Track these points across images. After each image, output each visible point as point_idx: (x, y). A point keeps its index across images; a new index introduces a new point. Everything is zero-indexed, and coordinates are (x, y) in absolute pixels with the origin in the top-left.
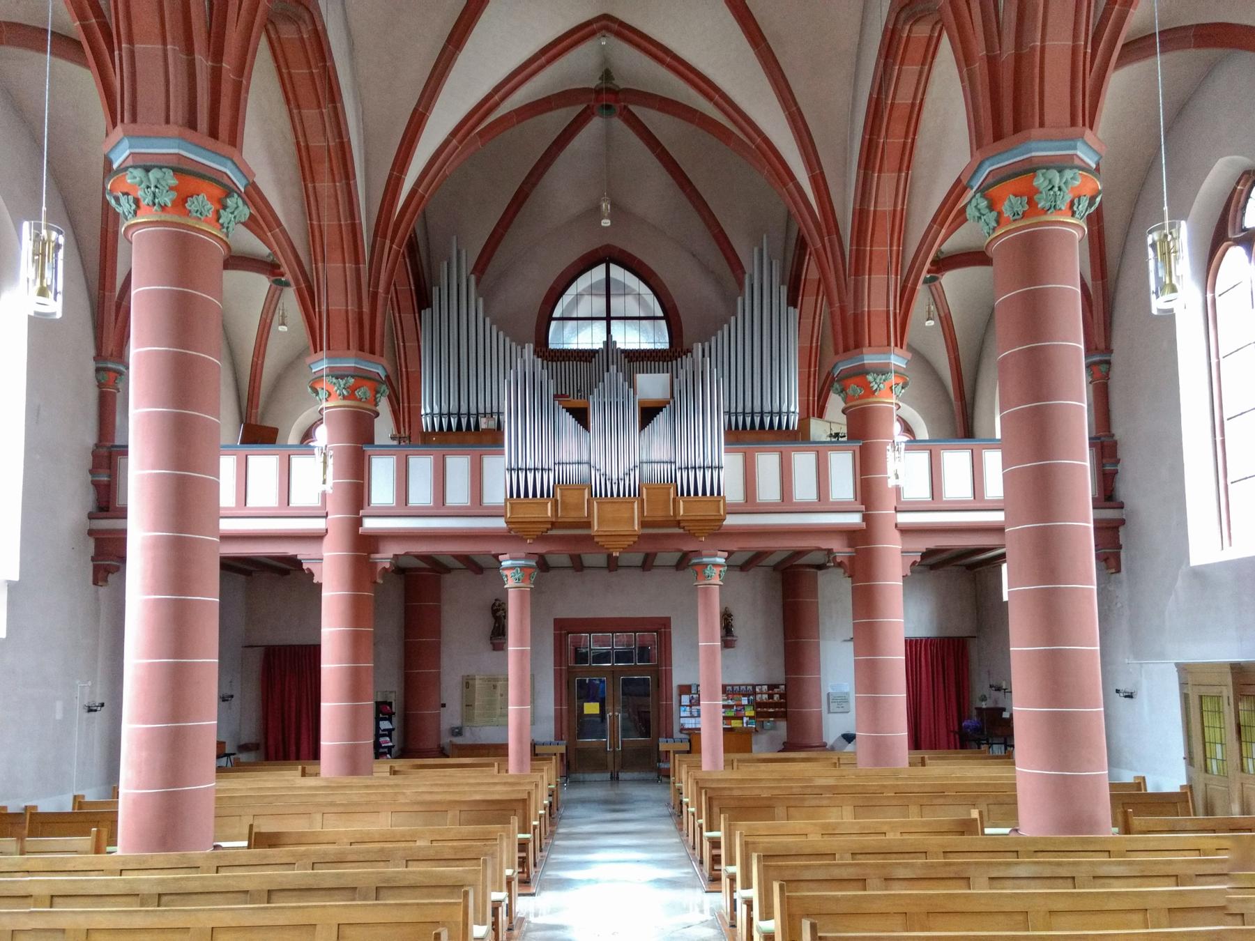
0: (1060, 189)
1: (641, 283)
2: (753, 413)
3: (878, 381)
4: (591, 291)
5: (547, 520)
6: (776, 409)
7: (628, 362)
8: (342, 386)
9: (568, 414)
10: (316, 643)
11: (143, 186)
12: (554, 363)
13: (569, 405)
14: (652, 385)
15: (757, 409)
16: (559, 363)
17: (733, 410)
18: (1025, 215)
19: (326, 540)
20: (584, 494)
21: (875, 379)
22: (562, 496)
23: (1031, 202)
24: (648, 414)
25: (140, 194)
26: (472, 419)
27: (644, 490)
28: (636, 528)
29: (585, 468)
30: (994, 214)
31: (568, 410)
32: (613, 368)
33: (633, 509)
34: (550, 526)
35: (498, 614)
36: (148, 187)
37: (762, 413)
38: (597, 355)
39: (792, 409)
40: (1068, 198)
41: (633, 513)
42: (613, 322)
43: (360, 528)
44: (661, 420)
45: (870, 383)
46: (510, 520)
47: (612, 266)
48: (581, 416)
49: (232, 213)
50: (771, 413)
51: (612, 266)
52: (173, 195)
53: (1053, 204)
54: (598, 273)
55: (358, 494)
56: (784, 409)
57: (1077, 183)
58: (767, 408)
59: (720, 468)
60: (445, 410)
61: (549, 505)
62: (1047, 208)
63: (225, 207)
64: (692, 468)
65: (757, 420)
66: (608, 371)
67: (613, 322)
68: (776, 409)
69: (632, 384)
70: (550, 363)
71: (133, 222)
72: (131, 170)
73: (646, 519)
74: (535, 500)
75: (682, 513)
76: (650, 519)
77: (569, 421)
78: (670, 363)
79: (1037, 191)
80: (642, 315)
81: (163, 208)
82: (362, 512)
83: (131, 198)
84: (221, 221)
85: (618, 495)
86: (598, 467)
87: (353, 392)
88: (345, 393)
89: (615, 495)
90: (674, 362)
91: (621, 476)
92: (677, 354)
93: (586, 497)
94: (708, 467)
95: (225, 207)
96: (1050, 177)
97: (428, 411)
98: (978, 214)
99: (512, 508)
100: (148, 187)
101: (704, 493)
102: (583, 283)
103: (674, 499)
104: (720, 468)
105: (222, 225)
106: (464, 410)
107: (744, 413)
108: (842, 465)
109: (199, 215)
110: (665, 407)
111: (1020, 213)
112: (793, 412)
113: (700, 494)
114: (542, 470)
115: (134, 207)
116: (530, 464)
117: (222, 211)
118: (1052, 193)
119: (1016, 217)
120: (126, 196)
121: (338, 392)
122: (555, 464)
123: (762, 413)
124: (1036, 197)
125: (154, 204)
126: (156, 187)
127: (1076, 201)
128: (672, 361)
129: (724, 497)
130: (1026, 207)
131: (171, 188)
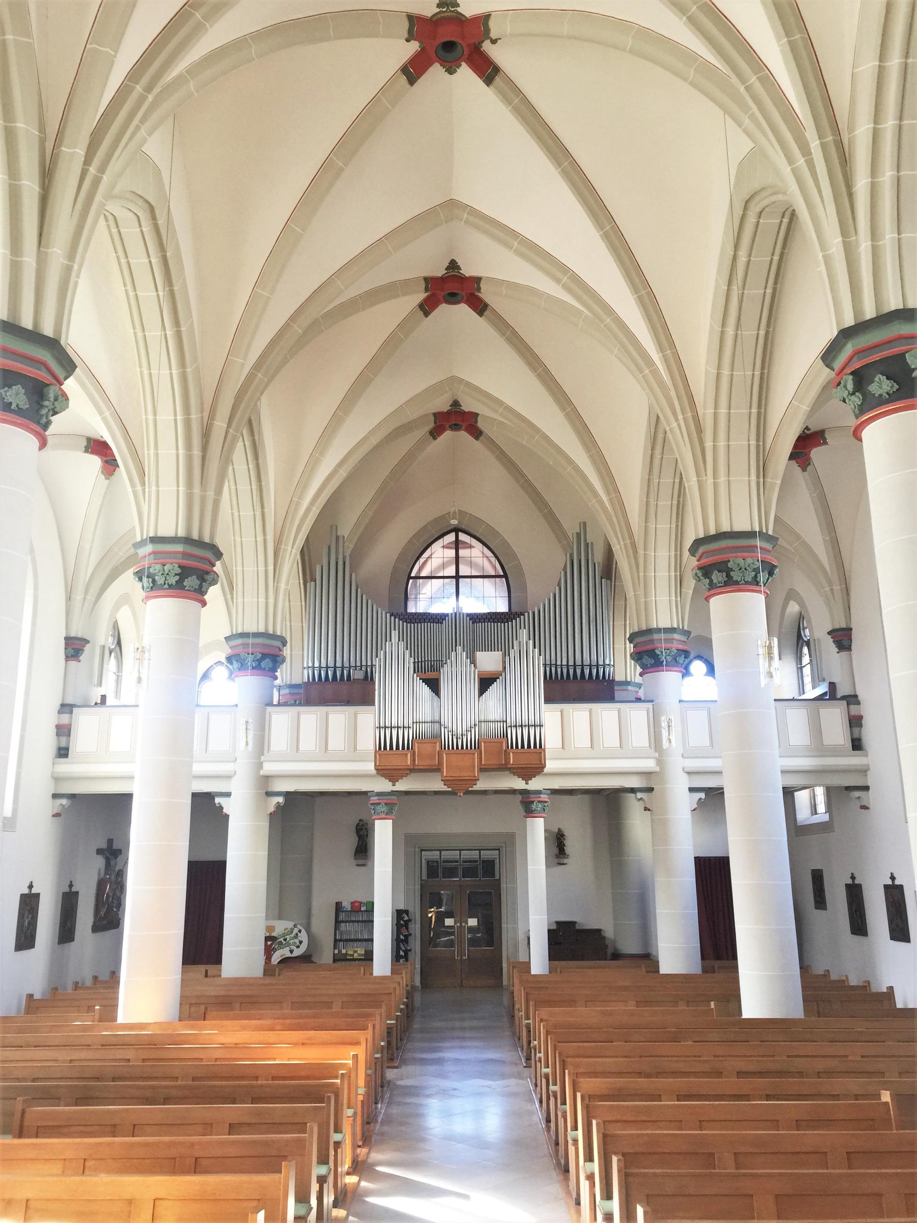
0: (746, 569)
1: (484, 547)
2: (575, 666)
6: (594, 663)
7: (473, 623)
10: (221, 859)
11: (160, 573)
12: (409, 625)
13: (424, 677)
14: (488, 661)
15: (579, 662)
16: (416, 624)
17: (559, 663)
19: (234, 779)
20: (436, 746)
23: (728, 576)
24: (485, 683)
25: (156, 578)
27: (483, 743)
30: (708, 581)
31: (424, 681)
32: (459, 649)
33: (474, 759)
35: (361, 833)
36: (162, 574)
37: (582, 666)
38: (447, 618)
39: (607, 662)
41: (474, 762)
43: (261, 771)
44: (495, 690)
45: (658, 655)
46: (380, 768)
48: (434, 685)
50: (590, 666)
51: (460, 534)
52: (177, 578)
53: (743, 578)
55: (261, 744)
56: (601, 663)
58: (587, 662)
59: (541, 726)
60: (323, 664)
61: (409, 755)
65: (579, 671)
68: (594, 663)
69: (473, 662)
70: (409, 625)
73: (483, 767)
74: (398, 752)
75: (511, 762)
77: (426, 690)
78: (506, 624)
79: (732, 570)
81: (170, 586)
82: (262, 758)
87: (259, 664)
88: (254, 665)
89: (460, 748)
90: (510, 623)
91: (465, 732)
92: (512, 616)
97: (310, 665)
101: (529, 746)
102: (437, 548)
104: (541, 726)
106: (339, 664)
110: (499, 678)
115: (151, 585)
118: (741, 571)
119: (720, 585)
122: (413, 723)
123: (582, 666)
124: (732, 573)
125: (165, 584)
128: (508, 622)
129: (544, 750)
130: (726, 579)
131: (176, 574)
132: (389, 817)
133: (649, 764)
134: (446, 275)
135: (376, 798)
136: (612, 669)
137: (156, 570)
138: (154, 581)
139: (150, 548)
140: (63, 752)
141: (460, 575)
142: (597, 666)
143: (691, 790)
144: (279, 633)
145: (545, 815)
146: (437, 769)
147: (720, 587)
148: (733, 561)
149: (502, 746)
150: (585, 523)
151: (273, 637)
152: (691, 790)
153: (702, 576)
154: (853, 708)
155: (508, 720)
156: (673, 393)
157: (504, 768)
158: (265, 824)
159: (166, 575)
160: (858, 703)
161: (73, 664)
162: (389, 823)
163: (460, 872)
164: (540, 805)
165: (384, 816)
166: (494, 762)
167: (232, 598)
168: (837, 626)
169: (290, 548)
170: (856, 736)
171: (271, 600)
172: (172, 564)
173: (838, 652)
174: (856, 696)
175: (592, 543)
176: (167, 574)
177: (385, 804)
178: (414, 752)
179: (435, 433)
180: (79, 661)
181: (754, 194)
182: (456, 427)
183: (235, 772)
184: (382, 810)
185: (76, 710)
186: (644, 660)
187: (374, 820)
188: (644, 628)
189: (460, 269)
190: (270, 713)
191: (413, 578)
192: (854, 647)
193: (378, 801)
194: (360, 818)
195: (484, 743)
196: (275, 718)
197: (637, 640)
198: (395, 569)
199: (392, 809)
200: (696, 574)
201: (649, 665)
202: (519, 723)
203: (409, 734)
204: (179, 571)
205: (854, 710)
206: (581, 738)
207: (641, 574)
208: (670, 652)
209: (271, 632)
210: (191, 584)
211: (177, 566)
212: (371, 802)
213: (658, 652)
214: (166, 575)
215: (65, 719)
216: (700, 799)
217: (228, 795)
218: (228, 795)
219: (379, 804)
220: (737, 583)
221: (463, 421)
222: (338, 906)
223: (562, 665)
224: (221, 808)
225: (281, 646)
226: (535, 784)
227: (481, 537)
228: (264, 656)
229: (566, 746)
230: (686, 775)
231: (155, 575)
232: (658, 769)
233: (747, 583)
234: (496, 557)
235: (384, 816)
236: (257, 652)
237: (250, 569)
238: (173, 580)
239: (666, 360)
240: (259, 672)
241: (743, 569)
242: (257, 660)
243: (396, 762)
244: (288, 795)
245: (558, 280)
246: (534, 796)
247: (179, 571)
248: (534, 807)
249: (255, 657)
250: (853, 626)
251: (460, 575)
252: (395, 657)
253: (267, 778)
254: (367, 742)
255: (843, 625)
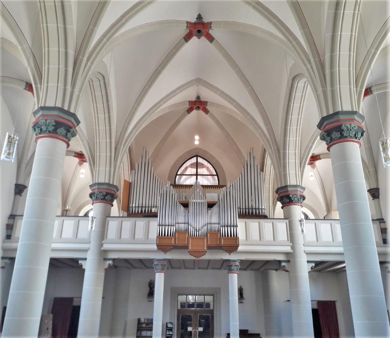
0: (351, 130)
2: (249, 209)
3: (294, 197)
4: (192, 166)
5: (172, 245)
6: (257, 207)
8: (101, 195)
9: (181, 205)
11: (44, 125)
18: (340, 138)
21: (293, 196)
22: (178, 236)
23: (341, 134)
24: (211, 205)
25: (43, 127)
26: (146, 209)
28: (205, 249)
29: (186, 225)
30: (329, 138)
33: (204, 241)
34: (172, 247)
38: (192, 187)
39: (263, 208)
40: (354, 133)
41: (204, 243)
42: (198, 176)
44: (215, 209)
45: (291, 197)
46: (158, 245)
47: (199, 158)
49: (71, 134)
50: (256, 209)
51: (199, 158)
52: (53, 128)
53: (349, 135)
54: (194, 160)
56: (260, 207)
57: (356, 129)
62: (347, 136)
63: (69, 132)
64: (226, 226)
66: (196, 190)
67: (198, 176)
68: (257, 207)
71: (39, 136)
72: (41, 120)
73: (209, 245)
74: (168, 237)
75: (222, 243)
76: (210, 245)
77: (182, 208)
79: (343, 130)
80: (209, 174)
81: (50, 132)
82: (103, 242)
83: (39, 129)
84: (67, 136)
85: (199, 236)
86: (191, 225)
93: (187, 236)
94: (232, 226)
95: (69, 132)
96: (347, 126)
98: (323, 138)
99: (159, 240)
100: (46, 125)
103: (220, 238)
105: (68, 138)
107: (245, 208)
108: (282, 227)
109: (60, 134)
111: (338, 137)
112: (264, 209)
113: (229, 236)
114: (171, 225)
115: (40, 131)
116: (167, 223)
117: (68, 133)
119: (337, 139)
120: (38, 128)
121: (99, 197)
122: (176, 223)
124: (343, 133)
125: (47, 131)
126: (48, 125)
127: (357, 134)
129: (238, 238)
130: (340, 136)
131: (53, 126)
132: (162, 271)
133: (288, 249)
134: (196, 22)
135: (157, 262)
136: (265, 211)
137: (42, 122)
138: (41, 130)
139: (40, 113)
140: (9, 237)
141: (198, 174)
142: (259, 209)
143: (308, 262)
144: (115, 184)
145: (237, 272)
146: (186, 247)
147: (337, 140)
148: (344, 125)
149: (218, 236)
150: (253, 148)
151: (113, 186)
152: (308, 262)
153: (326, 135)
154: (382, 224)
155: (221, 223)
156: (270, 142)
157: (219, 247)
158: (102, 274)
159: (47, 125)
160: (385, 222)
161: (18, 196)
162: (163, 275)
163: (196, 306)
164: (235, 267)
165: (160, 271)
166: (214, 243)
167: (94, 168)
168: (372, 187)
169: (122, 147)
170: (384, 238)
171: (112, 169)
172: (51, 119)
173: (373, 200)
174: (383, 219)
175: (256, 157)
176: (48, 125)
177: (161, 265)
178: (176, 237)
179: (190, 110)
180: (21, 196)
181: (297, 75)
182: (198, 108)
183: (89, 248)
184: (159, 268)
185: (16, 218)
186: (283, 200)
187: (155, 273)
188: (283, 185)
189: (202, 19)
190: (108, 221)
191: (179, 175)
192: (380, 197)
193: (158, 264)
194: (151, 279)
195: (209, 234)
196: (110, 223)
197: (280, 191)
198: (171, 172)
199: (164, 268)
200: (323, 135)
201: (286, 202)
202: (226, 224)
203: (173, 229)
204: (54, 124)
205: (383, 225)
206: (255, 235)
207: (282, 161)
208: (297, 196)
209: (111, 183)
210: (61, 132)
211: (53, 121)
212: (154, 264)
213: (291, 196)
214: (47, 125)
215: (11, 221)
216: (312, 266)
217: (85, 259)
218: (85, 259)
219: (158, 265)
220: (346, 137)
221: (201, 105)
222: (139, 320)
223: (243, 208)
224: (82, 266)
225: (116, 191)
226: (232, 257)
227: (207, 159)
228: (107, 194)
229: (248, 239)
230: (305, 255)
231: (42, 125)
232: (292, 251)
233: (351, 137)
234: (213, 167)
235: (160, 271)
236: (103, 192)
237: (103, 154)
238: (51, 129)
239: (268, 129)
240: (105, 201)
241: (349, 130)
242: (103, 196)
243: (166, 242)
244: (114, 260)
245: (232, 104)
246: (233, 262)
247: (54, 124)
248: (232, 268)
249: (102, 194)
250: (380, 187)
251: (198, 174)
252: (168, 201)
253: (106, 251)
254: (153, 235)
255: (375, 187)
